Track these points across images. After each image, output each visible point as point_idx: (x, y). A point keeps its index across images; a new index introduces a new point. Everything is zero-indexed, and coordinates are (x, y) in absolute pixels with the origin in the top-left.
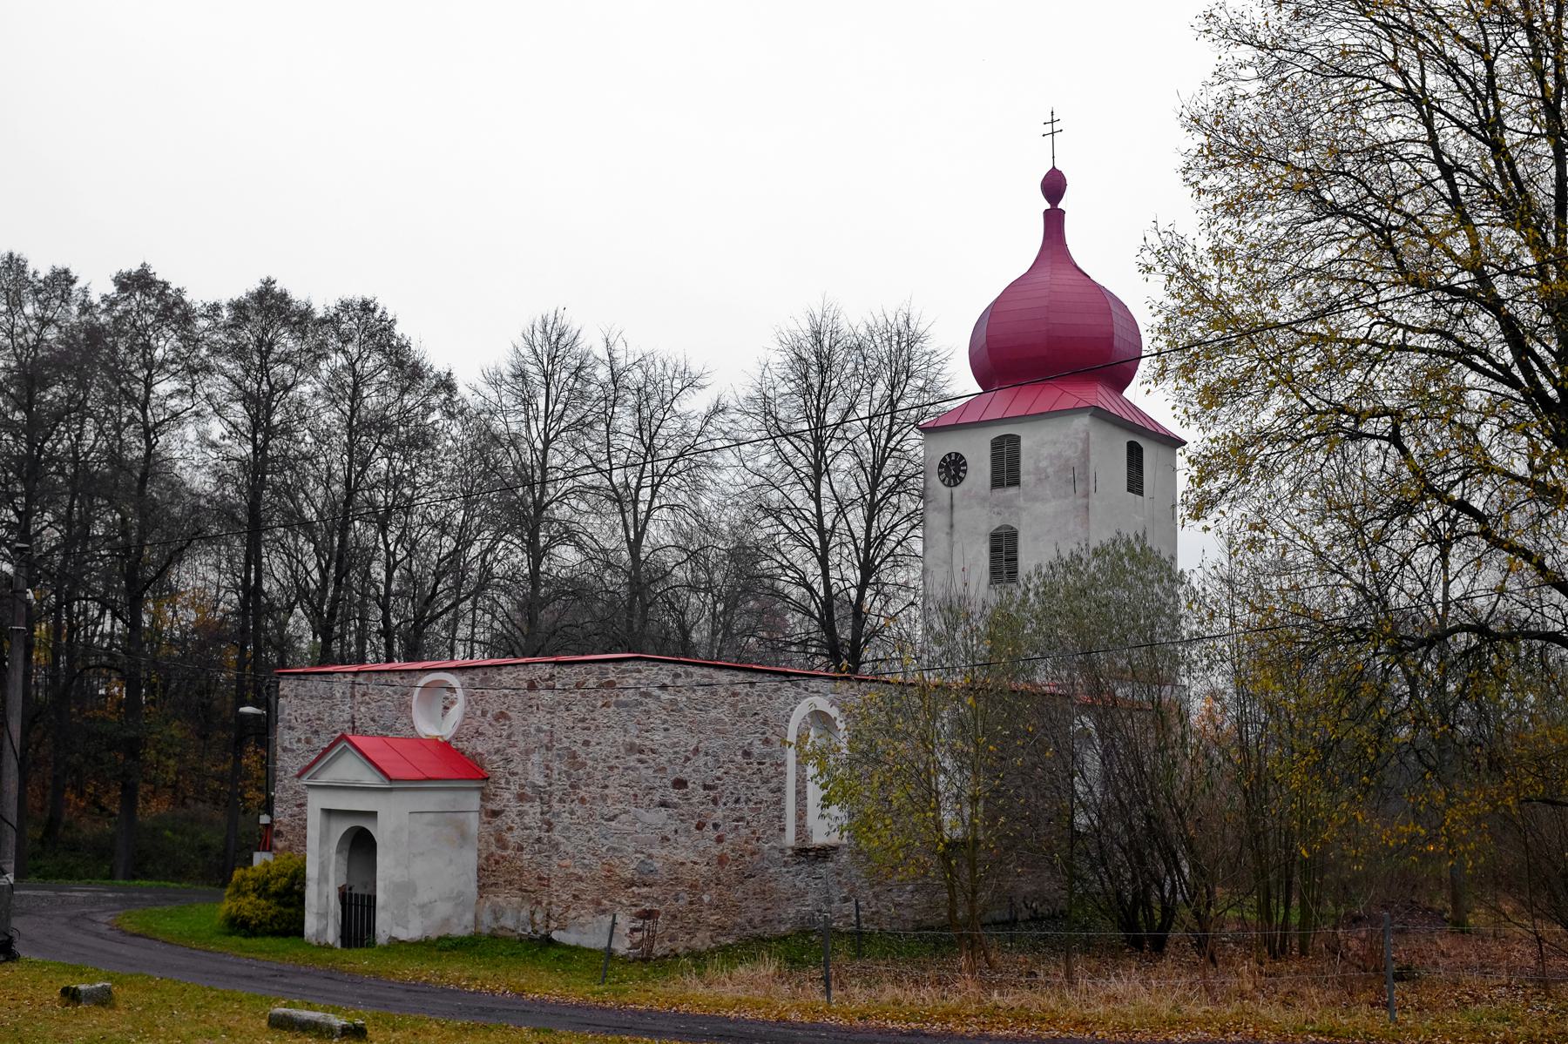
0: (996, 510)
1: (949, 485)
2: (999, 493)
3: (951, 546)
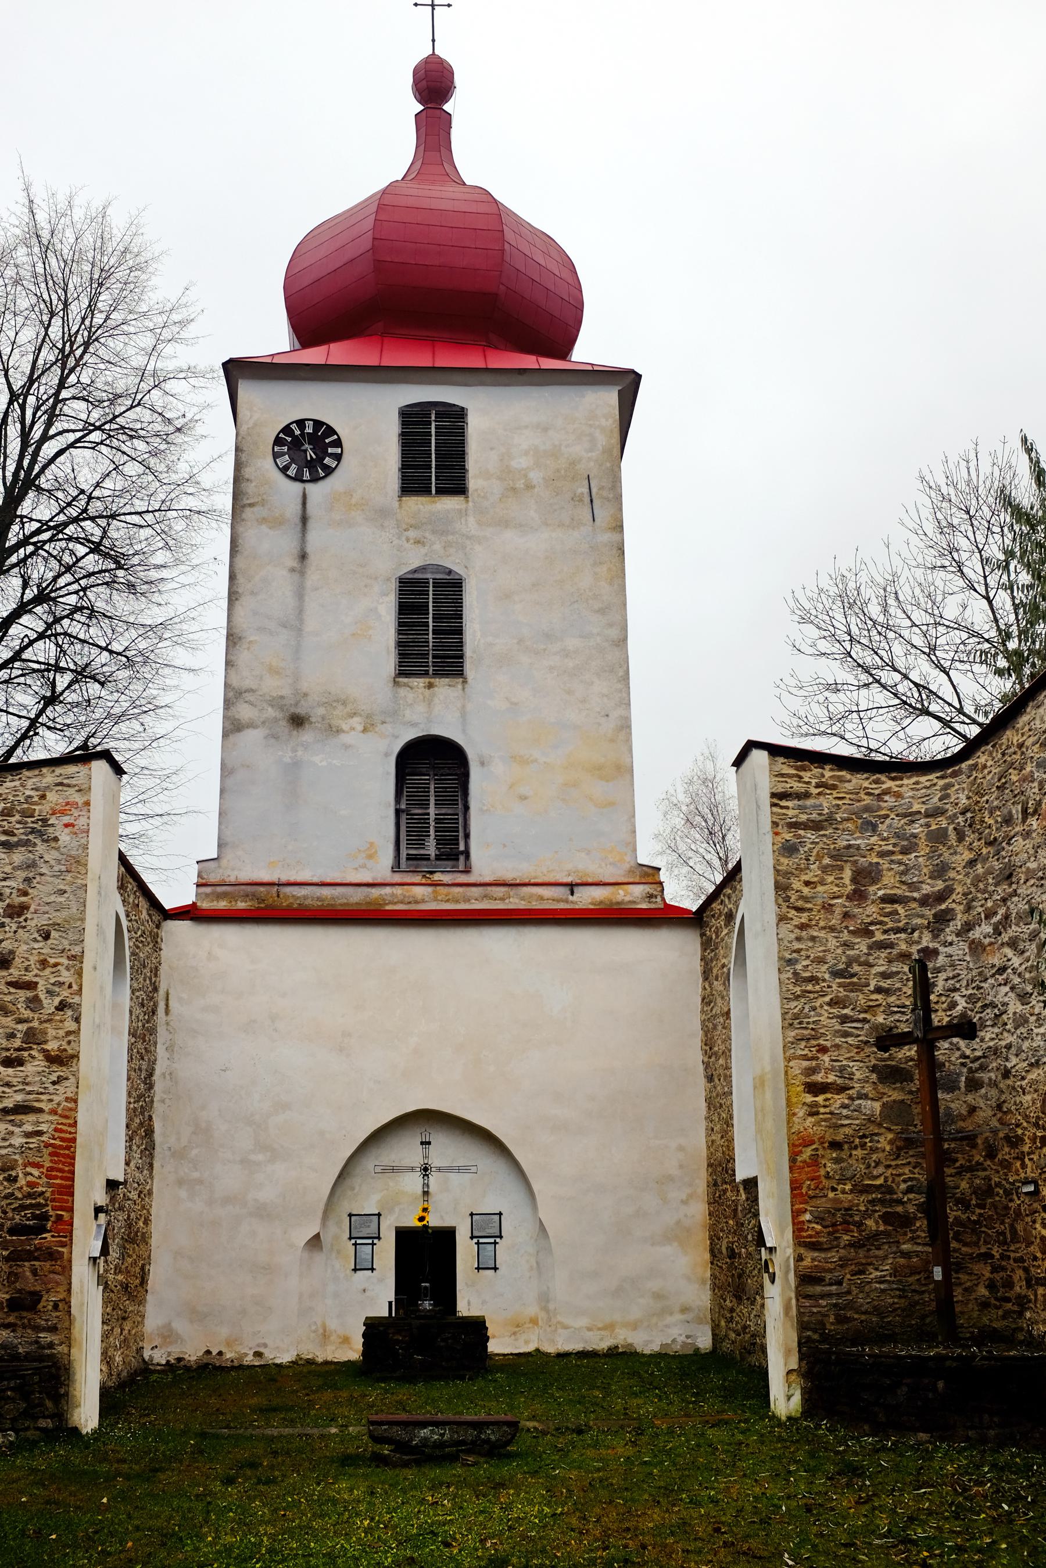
0: (412, 534)
1: (298, 478)
2: (415, 503)
3: (300, 594)
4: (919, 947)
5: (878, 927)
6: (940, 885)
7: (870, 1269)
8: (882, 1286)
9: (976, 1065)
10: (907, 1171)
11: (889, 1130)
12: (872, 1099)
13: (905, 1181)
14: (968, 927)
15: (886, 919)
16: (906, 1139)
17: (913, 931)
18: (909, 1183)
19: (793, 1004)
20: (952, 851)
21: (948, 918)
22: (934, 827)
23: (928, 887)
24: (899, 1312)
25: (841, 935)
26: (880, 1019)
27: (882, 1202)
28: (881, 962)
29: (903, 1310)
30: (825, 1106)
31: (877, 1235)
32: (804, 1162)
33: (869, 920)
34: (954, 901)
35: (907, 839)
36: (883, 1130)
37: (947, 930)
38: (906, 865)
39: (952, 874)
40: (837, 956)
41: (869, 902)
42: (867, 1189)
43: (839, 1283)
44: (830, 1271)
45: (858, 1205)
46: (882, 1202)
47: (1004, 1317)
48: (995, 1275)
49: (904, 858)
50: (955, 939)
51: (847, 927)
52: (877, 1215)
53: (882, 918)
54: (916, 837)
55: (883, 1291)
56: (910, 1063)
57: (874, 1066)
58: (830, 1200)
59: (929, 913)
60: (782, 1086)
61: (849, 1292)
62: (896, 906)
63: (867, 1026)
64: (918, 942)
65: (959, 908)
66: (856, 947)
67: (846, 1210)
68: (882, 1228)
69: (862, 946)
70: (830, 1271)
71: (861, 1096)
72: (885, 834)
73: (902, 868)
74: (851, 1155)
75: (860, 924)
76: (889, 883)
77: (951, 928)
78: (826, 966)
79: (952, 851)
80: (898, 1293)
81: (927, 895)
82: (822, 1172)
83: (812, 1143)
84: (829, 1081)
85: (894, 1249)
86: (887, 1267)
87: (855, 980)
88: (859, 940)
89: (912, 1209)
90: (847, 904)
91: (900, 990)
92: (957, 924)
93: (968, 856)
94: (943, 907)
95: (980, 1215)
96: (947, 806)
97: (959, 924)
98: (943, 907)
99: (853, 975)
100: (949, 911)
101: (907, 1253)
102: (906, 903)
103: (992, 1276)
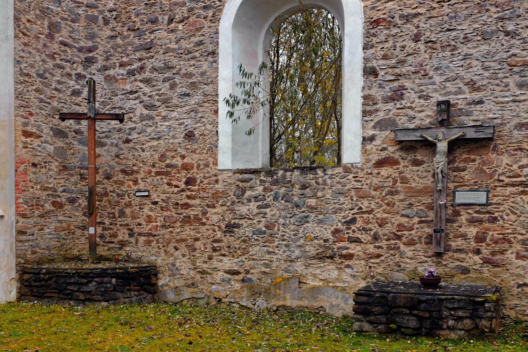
4: (76, 72)
5: (58, 56)
6: (90, 44)
7: (45, 228)
8: (50, 236)
9: (103, 135)
10: (63, 182)
11: (56, 160)
12: (50, 144)
13: (62, 186)
14: (106, 68)
15: (62, 53)
16: (64, 166)
17: (74, 63)
18: (64, 188)
19: (19, 86)
20: (99, 28)
21: (93, 61)
22: (89, 13)
23: (83, 43)
24: (57, 248)
25: (42, 55)
26: (55, 104)
27: (52, 195)
28: (58, 75)
29: (58, 248)
30: (31, 144)
31: (49, 212)
32: (21, 172)
33: (54, 51)
34: (97, 53)
35: (75, 15)
36: (53, 160)
37: (92, 67)
38: (73, 28)
39: (98, 40)
40: (40, 67)
41: (55, 42)
42: (46, 189)
43: (33, 235)
44: (30, 228)
45: (42, 196)
46: (52, 195)
47: (108, 250)
48: (105, 232)
49: (72, 24)
50: (96, 73)
51: (45, 52)
52: (50, 202)
53: (60, 52)
54: (79, 15)
55: (51, 238)
56: (67, 129)
57: (51, 128)
58: (31, 193)
59: (83, 56)
60: (13, 130)
61: (37, 239)
62: (67, 48)
63: (50, 106)
64: (76, 70)
65: (100, 58)
66: (48, 64)
67: (38, 198)
68: (52, 208)
69: (50, 64)
70: (30, 228)
71: (45, 143)
72: (64, 9)
73: (71, 29)
74: (40, 171)
75: (51, 52)
76: (63, 35)
77: (95, 67)
78: (35, 70)
79: (99, 28)
80: (57, 239)
81: (83, 47)
82: (28, 178)
83: (24, 162)
84: (33, 131)
85: (55, 219)
86: (52, 227)
87: (46, 81)
88: (49, 60)
89: (64, 200)
90: (46, 39)
91: (65, 91)
92: (99, 65)
93: (109, 33)
94: (91, 55)
95: (99, 205)
96: (99, 5)
97: (100, 66)
98: (91, 55)
99: (46, 78)
100: (93, 58)
101: (61, 221)
102: (71, 48)
103: (102, 232)
